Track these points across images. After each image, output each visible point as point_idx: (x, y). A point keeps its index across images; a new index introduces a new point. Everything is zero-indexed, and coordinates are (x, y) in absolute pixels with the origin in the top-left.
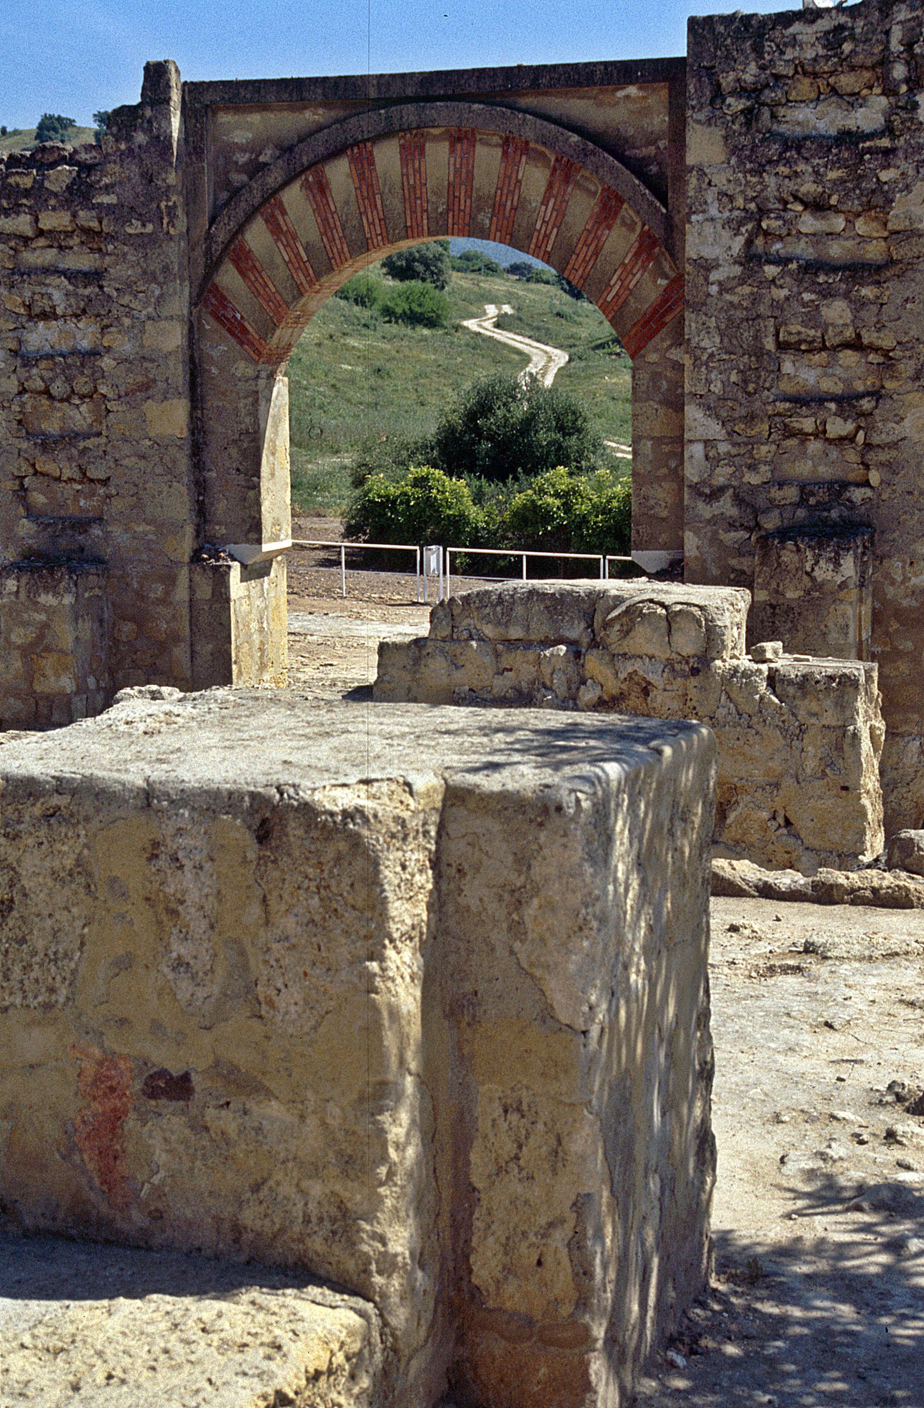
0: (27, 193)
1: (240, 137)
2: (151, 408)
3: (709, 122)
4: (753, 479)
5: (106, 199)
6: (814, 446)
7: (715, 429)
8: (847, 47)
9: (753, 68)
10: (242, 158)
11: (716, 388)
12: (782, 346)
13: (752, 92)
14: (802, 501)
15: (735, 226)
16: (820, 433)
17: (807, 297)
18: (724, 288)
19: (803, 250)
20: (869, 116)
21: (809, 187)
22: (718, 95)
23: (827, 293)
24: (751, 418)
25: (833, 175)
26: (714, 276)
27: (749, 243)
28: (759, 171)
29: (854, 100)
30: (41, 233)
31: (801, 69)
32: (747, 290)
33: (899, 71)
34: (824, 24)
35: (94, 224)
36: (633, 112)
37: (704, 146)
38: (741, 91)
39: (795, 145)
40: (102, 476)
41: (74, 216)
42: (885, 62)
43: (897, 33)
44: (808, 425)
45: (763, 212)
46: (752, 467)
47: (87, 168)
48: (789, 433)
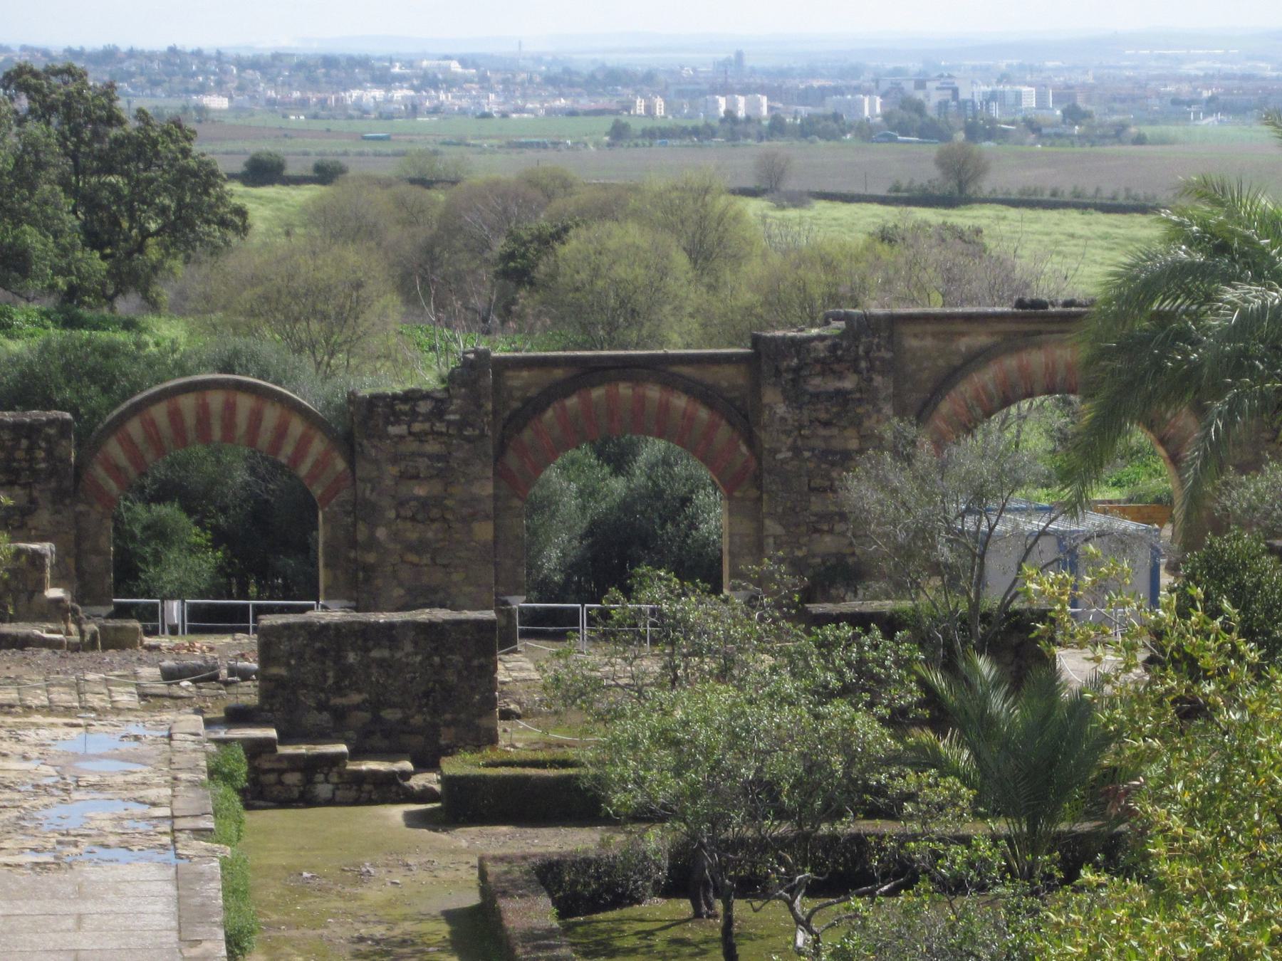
0: (405, 414)
1: (516, 383)
2: (476, 526)
3: (775, 385)
4: (799, 553)
5: (452, 417)
6: (828, 539)
7: (779, 530)
8: (839, 353)
9: (796, 360)
10: (518, 394)
11: (780, 510)
12: (812, 489)
13: (797, 370)
14: (824, 563)
15: (788, 433)
16: (831, 531)
17: (823, 466)
18: (783, 462)
19: (820, 444)
20: (848, 383)
21: (823, 416)
22: (778, 373)
23: (833, 464)
24: (797, 525)
25: (834, 410)
26: (780, 456)
27: (795, 441)
28: (800, 408)
29: (840, 376)
30: (410, 433)
31: (817, 360)
32: (795, 463)
33: (863, 364)
34: (828, 342)
35: (444, 430)
36: (727, 377)
37: (772, 397)
38: (789, 369)
39: (816, 396)
40: (445, 562)
41: (433, 425)
42: (856, 360)
43: (861, 349)
44: (826, 528)
45: (801, 427)
46: (800, 548)
47: (441, 401)
48: (817, 531)
